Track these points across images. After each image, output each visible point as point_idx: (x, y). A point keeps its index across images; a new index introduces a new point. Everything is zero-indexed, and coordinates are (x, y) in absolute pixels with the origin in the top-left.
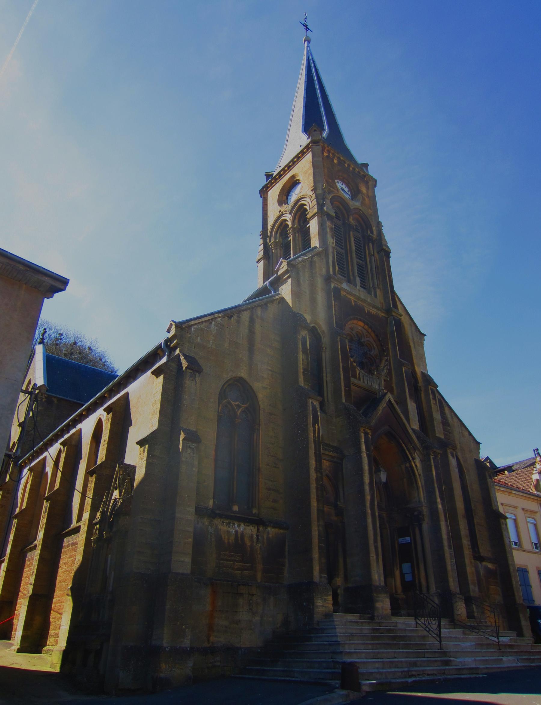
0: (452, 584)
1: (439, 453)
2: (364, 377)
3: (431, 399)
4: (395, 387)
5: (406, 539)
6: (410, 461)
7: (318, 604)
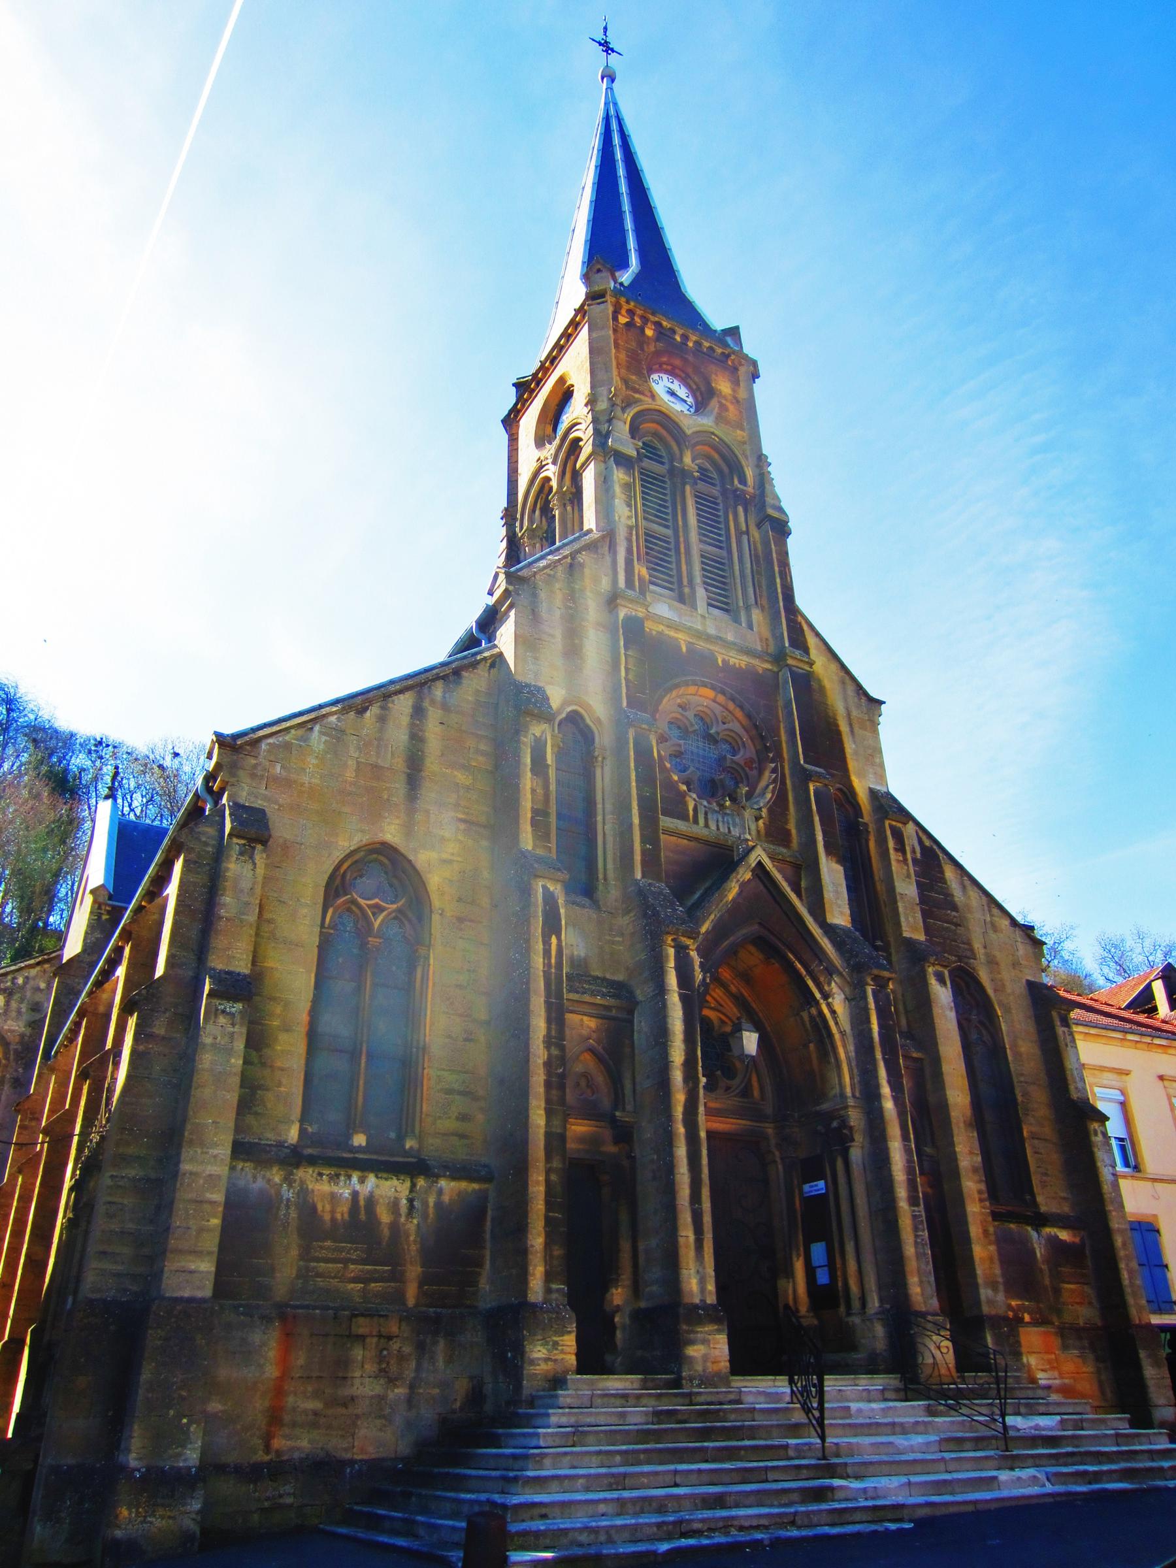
0: (918, 1290)
1: (889, 979)
2: (710, 816)
3: (892, 851)
4: (794, 832)
5: (816, 1185)
6: (817, 1003)
7: (536, 1355)
